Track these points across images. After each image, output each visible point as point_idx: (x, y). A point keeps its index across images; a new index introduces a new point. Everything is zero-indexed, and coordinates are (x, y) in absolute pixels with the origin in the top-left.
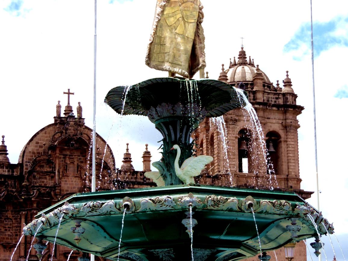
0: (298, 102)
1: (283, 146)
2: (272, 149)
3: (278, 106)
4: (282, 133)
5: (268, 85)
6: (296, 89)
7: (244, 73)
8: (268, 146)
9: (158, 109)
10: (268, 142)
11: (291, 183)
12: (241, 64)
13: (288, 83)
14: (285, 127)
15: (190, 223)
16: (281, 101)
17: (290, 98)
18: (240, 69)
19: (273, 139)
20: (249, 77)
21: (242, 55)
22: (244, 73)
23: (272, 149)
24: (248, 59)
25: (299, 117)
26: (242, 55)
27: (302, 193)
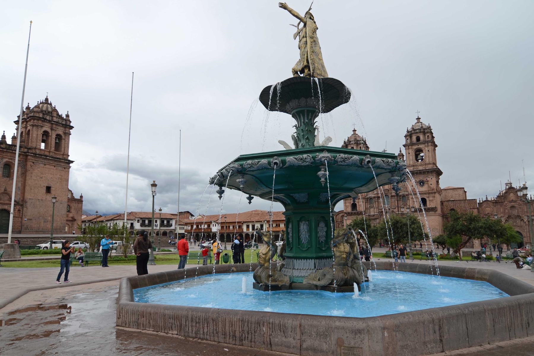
0: (71, 125)
1: (63, 141)
2: (57, 141)
3: (63, 124)
4: (63, 136)
5: (58, 114)
6: (71, 118)
7: (47, 108)
8: (56, 140)
9: (290, 104)
10: (56, 138)
11: (65, 156)
12: (46, 103)
13: (67, 116)
14: (65, 133)
15: (324, 173)
16: (64, 123)
17: (68, 122)
18: (45, 105)
19: (59, 137)
20: (50, 110)
21: (47, 99)
22: (47, 108)
23: (57, 141)
24: (49, 102)
25: (71, 131)
26: (47, 99)
27: (69, 161)
